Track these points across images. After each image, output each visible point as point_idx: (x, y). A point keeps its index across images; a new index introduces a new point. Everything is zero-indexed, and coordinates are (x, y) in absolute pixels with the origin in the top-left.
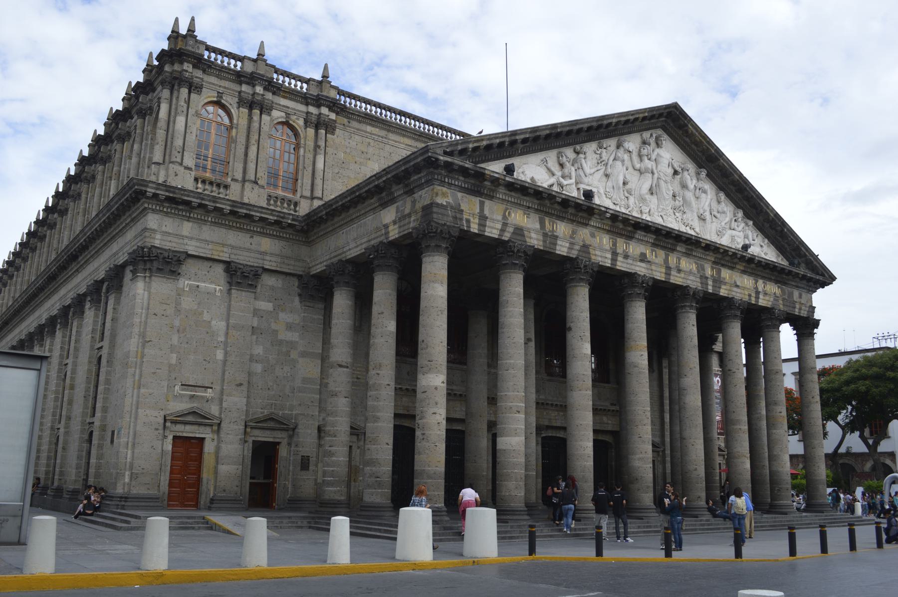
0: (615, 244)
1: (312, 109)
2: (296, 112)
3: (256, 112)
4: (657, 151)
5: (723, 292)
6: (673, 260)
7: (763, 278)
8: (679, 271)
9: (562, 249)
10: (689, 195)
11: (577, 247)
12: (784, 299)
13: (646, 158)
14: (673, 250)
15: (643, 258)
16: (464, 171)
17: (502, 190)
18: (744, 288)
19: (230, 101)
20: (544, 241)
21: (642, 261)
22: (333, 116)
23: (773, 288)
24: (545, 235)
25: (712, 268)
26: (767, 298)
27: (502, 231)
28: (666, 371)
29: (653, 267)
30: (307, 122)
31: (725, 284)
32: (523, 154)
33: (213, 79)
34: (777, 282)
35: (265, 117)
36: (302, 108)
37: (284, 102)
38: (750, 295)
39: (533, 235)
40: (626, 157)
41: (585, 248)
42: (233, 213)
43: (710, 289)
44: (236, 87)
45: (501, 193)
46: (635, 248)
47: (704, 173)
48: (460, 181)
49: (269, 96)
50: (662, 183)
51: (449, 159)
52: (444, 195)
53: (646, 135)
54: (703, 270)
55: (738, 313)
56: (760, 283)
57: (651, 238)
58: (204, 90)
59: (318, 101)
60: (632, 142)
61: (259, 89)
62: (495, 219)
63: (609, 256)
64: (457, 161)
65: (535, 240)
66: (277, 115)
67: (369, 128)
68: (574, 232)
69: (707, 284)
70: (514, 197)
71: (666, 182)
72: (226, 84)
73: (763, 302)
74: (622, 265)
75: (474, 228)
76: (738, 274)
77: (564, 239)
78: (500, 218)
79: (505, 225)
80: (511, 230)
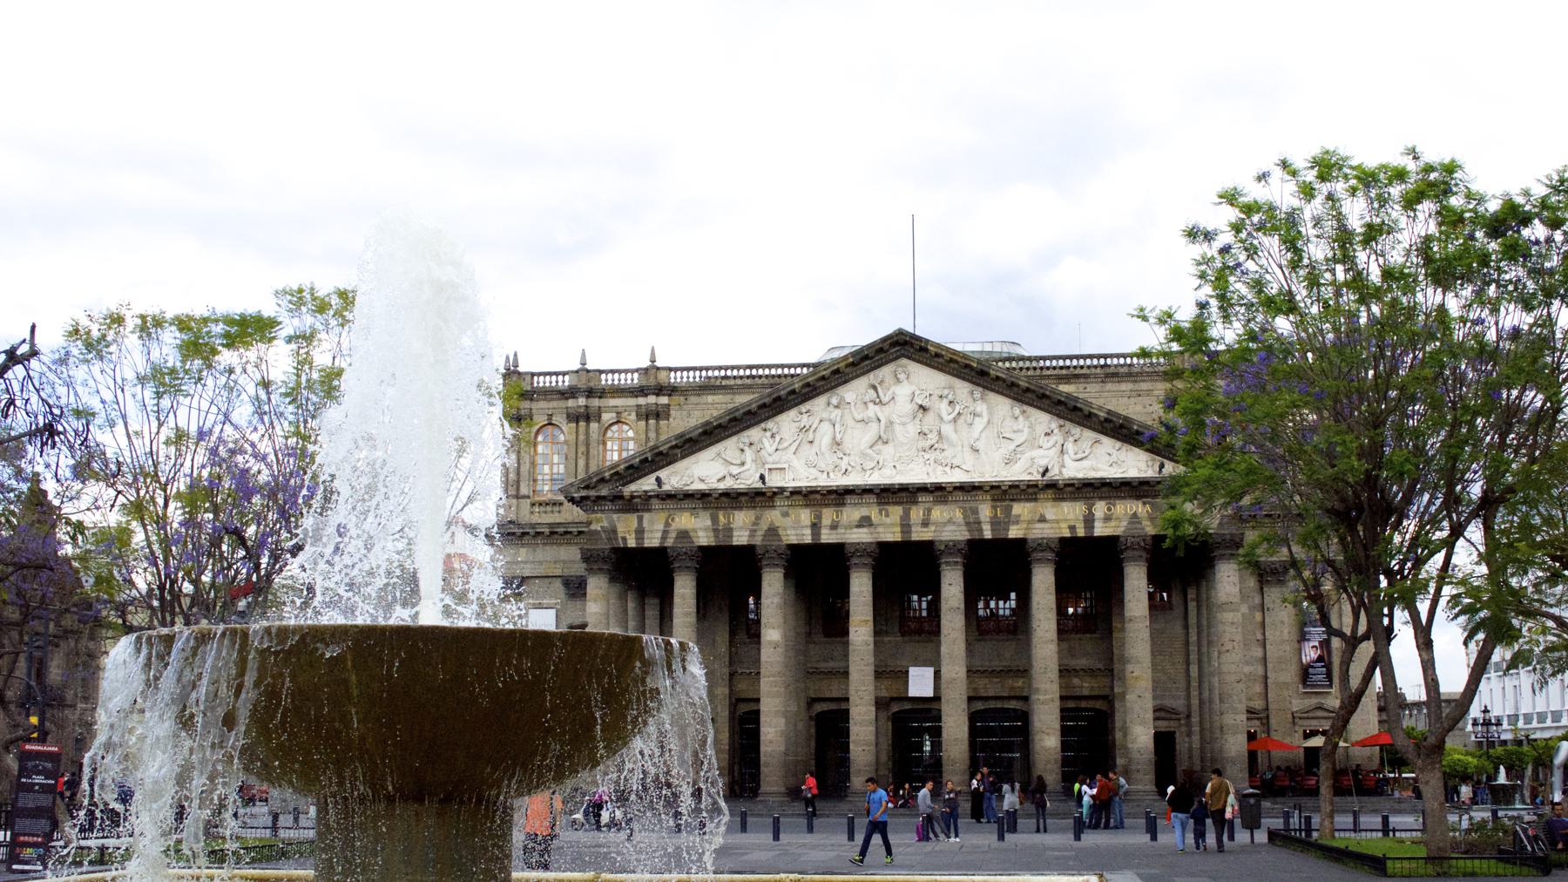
0: (819, 517)
1: (641, 401)
2: (626, 408)
3: (582, 424)
4: (893, 388)
5: (1014, 532)
6: (917, 514)
7: (1101, 498)
8: (925, 524)
9: (740, 538)
10: (947, 429)
11: (760, 533)
12: (1152, 519)
13: (871, 405)
14: (916, 502)
15: (865, 522)
16: (604, 498)
17: (654, 501)
18: (1057, 521)
19: (559, 419)
20: (716, 537)
21: (859, 526)
22: (664, 400)
23: (1126, 509)
24: (716, 531)
25: (994, 508)
26: (1113, 524)
27: (664, 538)
28: (1192, 605)
29: (880, 529)
30: (639, 416)
31: (1017, 522)
32: (683, 457)
33: (542, 404)
34: (1138, 498)
35: (594, 426)
36: (632, 402)
37: (613, 402)
38: (1072, 528)
39: (701, 534)
40: (836, 413)
41: (773, 531)
42: (552, 533)
43: (988, 534)
44: (562, 404)
45: (656, 504)
46: (852, 513)
47: (978, 391)
48: (609, 506)
49: (595, 402)
50: (897, 428)
51: (584, 493)
52: (598, 521)
53: (872, 377)
54: (975, 512)
55: (1050, 556)
56: (1100, 508)
57: (872, 499)
58: (535, 418)
59: (641, 391)
60: (854, 391)
61: (582, 401)
62: (654, 531)
63: (808, 531)
64: (592, 493)
65: (704, 539)
66: (607, 417)
67: (710, 398)
68: (758, 518)
69: (981, 530)
70: (670, 504)
71: (904, 424)
72: (554, 404)
73: (1100, 530)
74: (827, 537)
75: (632, 543)
76: (1049, 504)
77: (741, 528)
78: (661, 527)
79: (665, 532)
80: (673, 535)
